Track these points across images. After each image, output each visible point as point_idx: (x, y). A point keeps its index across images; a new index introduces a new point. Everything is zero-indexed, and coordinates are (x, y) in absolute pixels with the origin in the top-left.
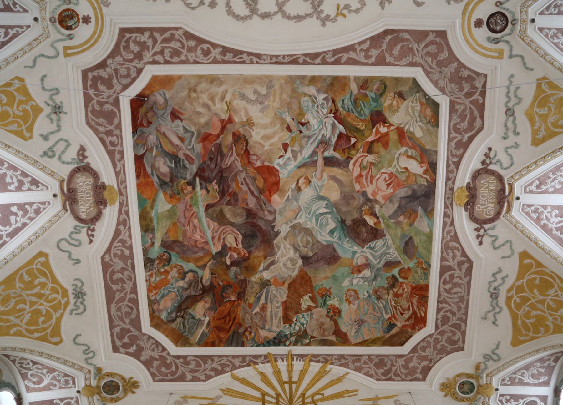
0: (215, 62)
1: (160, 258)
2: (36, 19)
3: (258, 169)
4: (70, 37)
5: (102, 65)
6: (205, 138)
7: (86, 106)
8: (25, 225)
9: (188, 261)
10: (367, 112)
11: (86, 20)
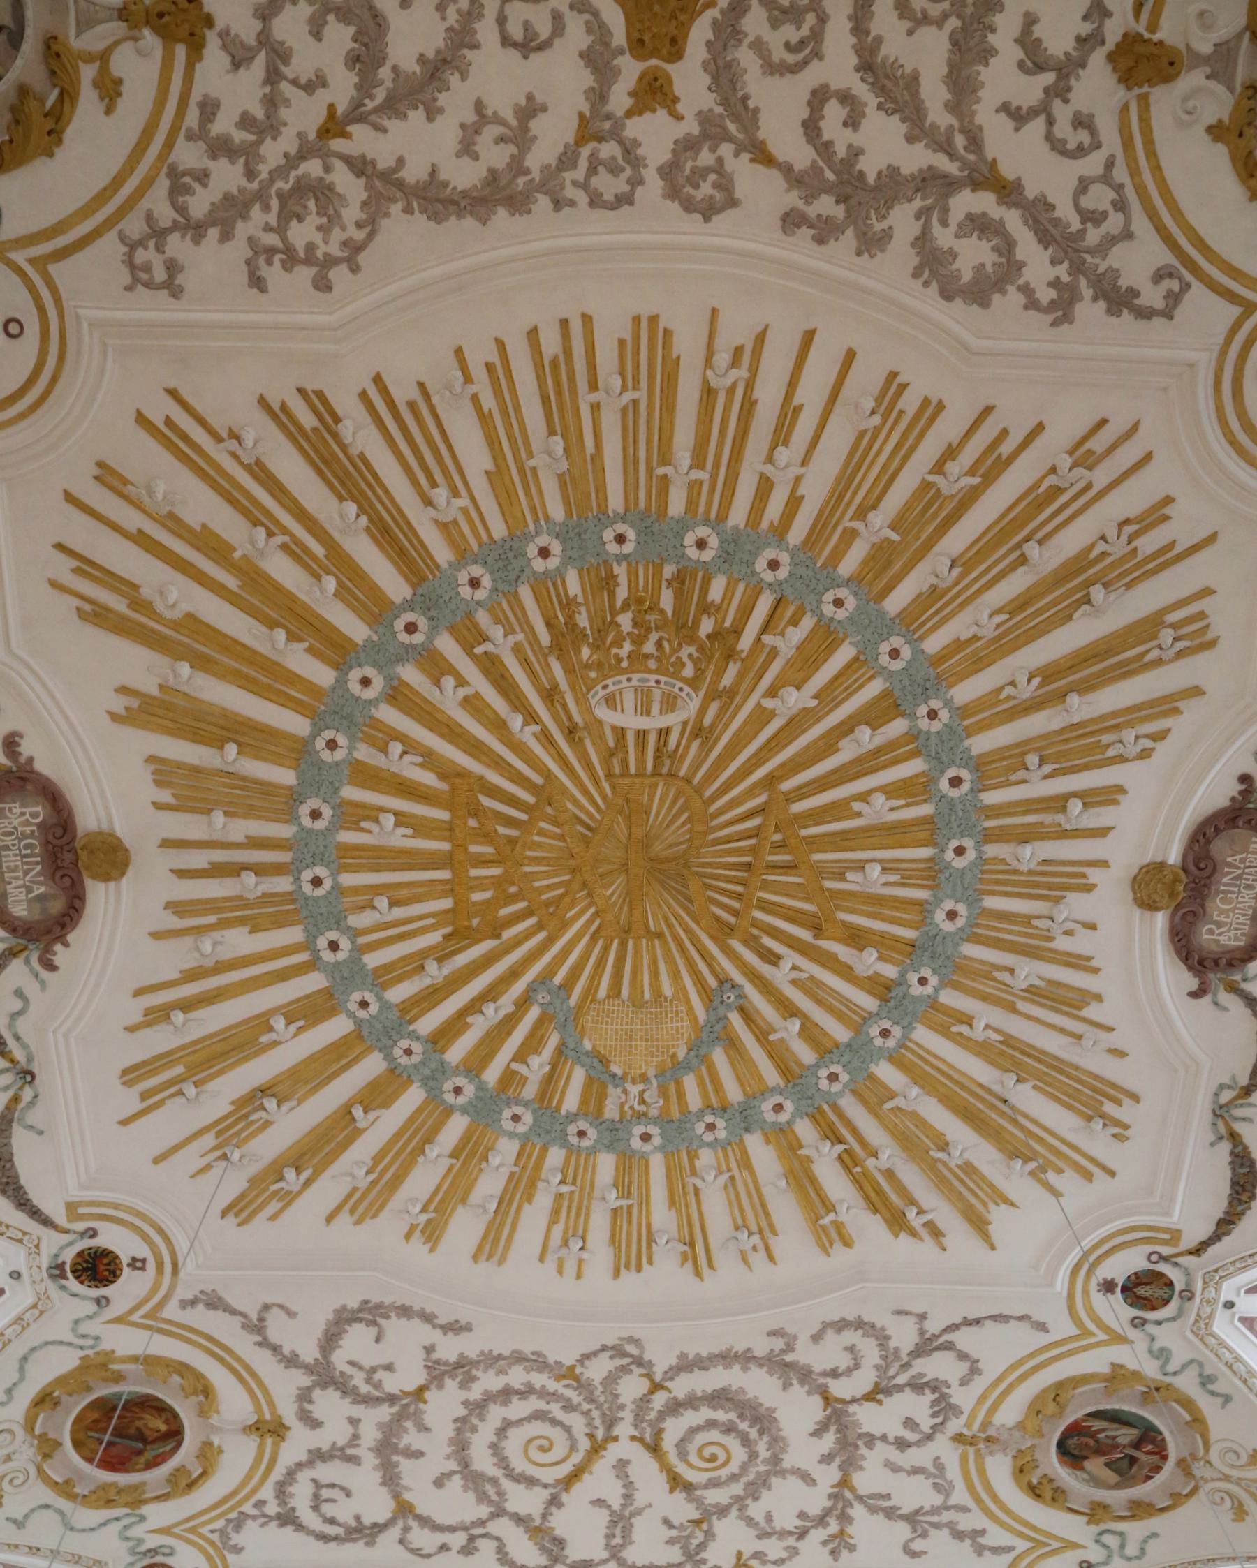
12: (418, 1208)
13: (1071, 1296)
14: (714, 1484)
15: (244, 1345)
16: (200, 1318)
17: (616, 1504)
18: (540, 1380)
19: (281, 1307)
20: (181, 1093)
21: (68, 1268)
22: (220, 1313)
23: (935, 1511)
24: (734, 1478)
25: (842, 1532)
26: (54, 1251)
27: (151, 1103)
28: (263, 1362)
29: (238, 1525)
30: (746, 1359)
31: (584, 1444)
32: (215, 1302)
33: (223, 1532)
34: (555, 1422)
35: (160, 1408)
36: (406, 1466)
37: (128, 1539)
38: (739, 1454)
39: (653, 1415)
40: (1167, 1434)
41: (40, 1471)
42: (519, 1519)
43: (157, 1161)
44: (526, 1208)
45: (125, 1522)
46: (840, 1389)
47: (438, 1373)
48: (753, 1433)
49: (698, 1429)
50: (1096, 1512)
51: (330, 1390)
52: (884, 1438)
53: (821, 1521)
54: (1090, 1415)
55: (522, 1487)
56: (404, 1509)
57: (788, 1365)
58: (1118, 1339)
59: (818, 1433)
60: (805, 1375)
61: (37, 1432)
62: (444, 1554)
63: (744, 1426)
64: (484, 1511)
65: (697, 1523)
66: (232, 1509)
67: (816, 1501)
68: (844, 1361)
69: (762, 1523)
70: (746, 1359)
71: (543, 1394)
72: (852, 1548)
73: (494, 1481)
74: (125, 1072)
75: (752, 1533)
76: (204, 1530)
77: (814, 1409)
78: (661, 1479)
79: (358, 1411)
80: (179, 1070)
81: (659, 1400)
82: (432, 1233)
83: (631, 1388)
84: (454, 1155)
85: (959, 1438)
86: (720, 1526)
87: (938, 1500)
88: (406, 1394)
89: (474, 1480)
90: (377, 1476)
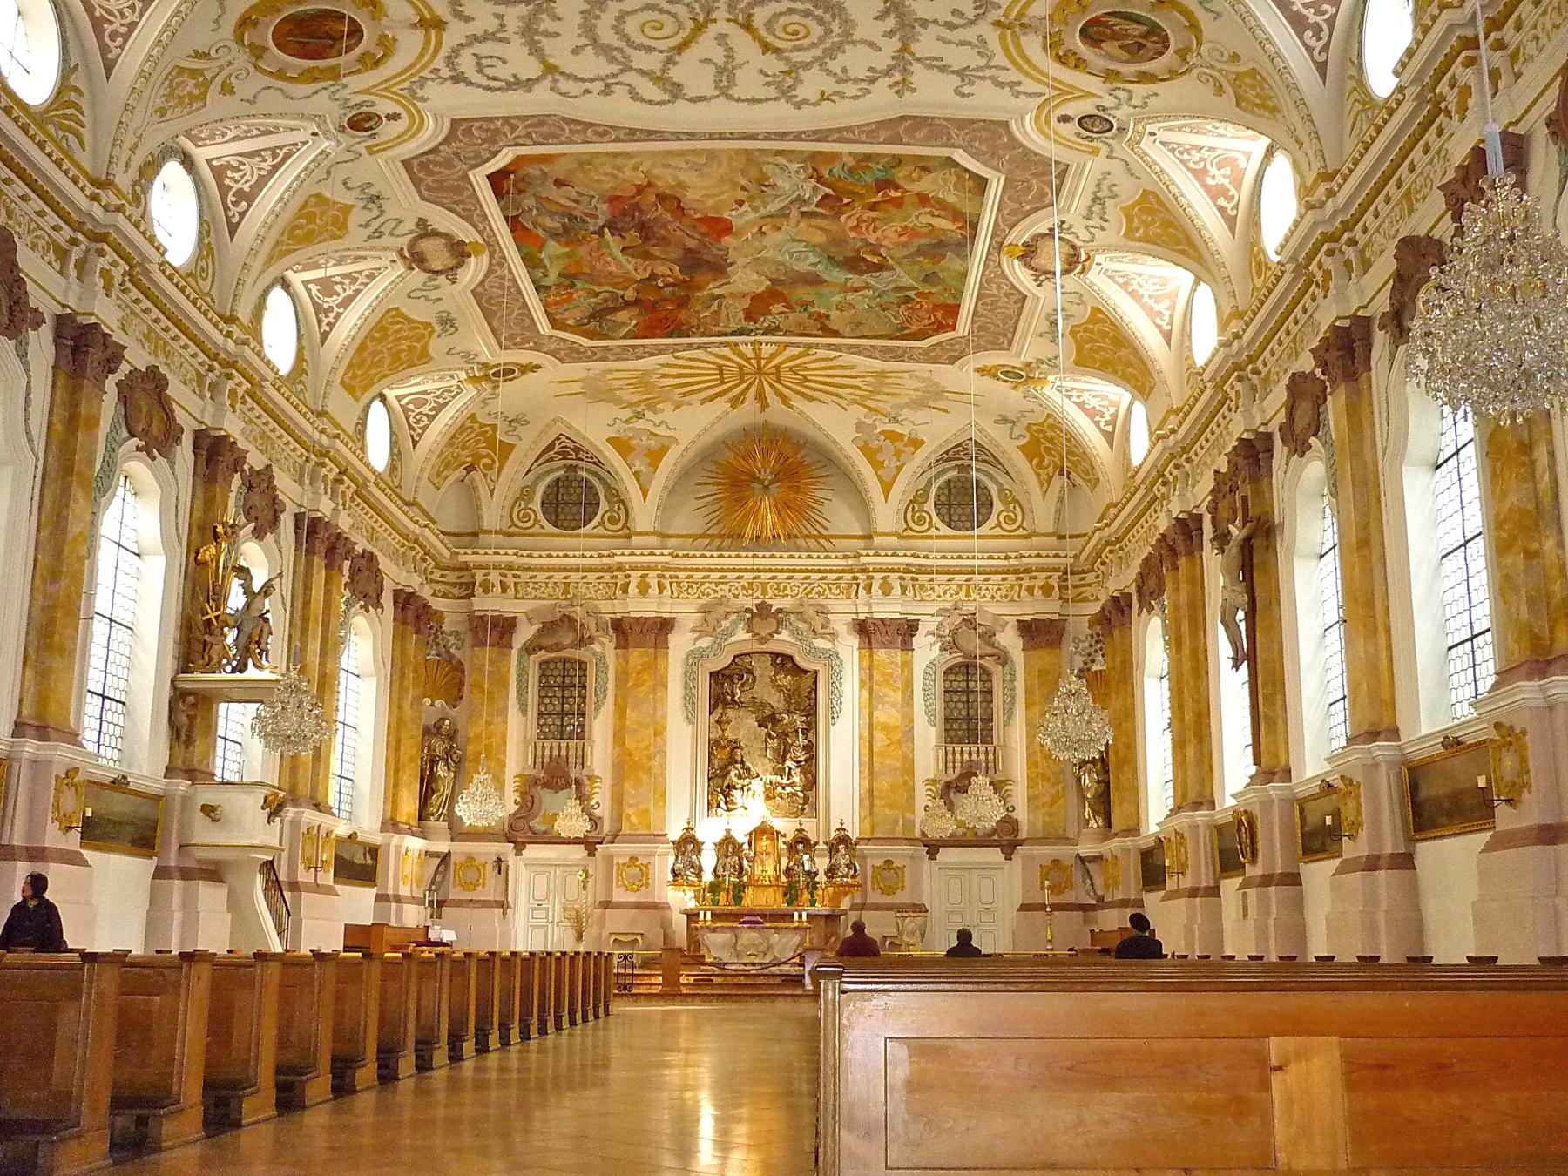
0: (617, 140)
1: (559, 285)
2: (314, 134)
3: (698, 219)
4: (373, 136)
5: (434, 150)
6: (612, 200)
7: (417, 187)
8: (358, 292)
9: (600, 284)
10: (869, 179)
11: (394, 117)
14: (798, 49)
17: (720, 61)
23: (979, 69)
24: (814, 45)
25: (904, 80)
29: (423, 82)
31: (691, 25)
33: (410, 89)
34: (661, 11)
36: (546, 43)
38: (817, 31)
40: (1169, 32)
42: (643, 73)
45: (332, 89)
48: (827, 17)
49: (781, 14)
50: (1110, 76)
52: (935, 21)
53: (888, 72)
54: (1109, 14)
56: (550, 69)
59: (882, 16)
63: (819, 12)
64: (615, 68)
65: (787, 73)
66: (412, 75)
67: (883, 60)
69: (839, 73)
72: (914, 90)
73: (620, 50)
76: (394, 89)
78: (755, 48)
85: (997, 24)
86: (804, 75)
87: (983, 62)
89: (605, 50)
90: (526, 49)
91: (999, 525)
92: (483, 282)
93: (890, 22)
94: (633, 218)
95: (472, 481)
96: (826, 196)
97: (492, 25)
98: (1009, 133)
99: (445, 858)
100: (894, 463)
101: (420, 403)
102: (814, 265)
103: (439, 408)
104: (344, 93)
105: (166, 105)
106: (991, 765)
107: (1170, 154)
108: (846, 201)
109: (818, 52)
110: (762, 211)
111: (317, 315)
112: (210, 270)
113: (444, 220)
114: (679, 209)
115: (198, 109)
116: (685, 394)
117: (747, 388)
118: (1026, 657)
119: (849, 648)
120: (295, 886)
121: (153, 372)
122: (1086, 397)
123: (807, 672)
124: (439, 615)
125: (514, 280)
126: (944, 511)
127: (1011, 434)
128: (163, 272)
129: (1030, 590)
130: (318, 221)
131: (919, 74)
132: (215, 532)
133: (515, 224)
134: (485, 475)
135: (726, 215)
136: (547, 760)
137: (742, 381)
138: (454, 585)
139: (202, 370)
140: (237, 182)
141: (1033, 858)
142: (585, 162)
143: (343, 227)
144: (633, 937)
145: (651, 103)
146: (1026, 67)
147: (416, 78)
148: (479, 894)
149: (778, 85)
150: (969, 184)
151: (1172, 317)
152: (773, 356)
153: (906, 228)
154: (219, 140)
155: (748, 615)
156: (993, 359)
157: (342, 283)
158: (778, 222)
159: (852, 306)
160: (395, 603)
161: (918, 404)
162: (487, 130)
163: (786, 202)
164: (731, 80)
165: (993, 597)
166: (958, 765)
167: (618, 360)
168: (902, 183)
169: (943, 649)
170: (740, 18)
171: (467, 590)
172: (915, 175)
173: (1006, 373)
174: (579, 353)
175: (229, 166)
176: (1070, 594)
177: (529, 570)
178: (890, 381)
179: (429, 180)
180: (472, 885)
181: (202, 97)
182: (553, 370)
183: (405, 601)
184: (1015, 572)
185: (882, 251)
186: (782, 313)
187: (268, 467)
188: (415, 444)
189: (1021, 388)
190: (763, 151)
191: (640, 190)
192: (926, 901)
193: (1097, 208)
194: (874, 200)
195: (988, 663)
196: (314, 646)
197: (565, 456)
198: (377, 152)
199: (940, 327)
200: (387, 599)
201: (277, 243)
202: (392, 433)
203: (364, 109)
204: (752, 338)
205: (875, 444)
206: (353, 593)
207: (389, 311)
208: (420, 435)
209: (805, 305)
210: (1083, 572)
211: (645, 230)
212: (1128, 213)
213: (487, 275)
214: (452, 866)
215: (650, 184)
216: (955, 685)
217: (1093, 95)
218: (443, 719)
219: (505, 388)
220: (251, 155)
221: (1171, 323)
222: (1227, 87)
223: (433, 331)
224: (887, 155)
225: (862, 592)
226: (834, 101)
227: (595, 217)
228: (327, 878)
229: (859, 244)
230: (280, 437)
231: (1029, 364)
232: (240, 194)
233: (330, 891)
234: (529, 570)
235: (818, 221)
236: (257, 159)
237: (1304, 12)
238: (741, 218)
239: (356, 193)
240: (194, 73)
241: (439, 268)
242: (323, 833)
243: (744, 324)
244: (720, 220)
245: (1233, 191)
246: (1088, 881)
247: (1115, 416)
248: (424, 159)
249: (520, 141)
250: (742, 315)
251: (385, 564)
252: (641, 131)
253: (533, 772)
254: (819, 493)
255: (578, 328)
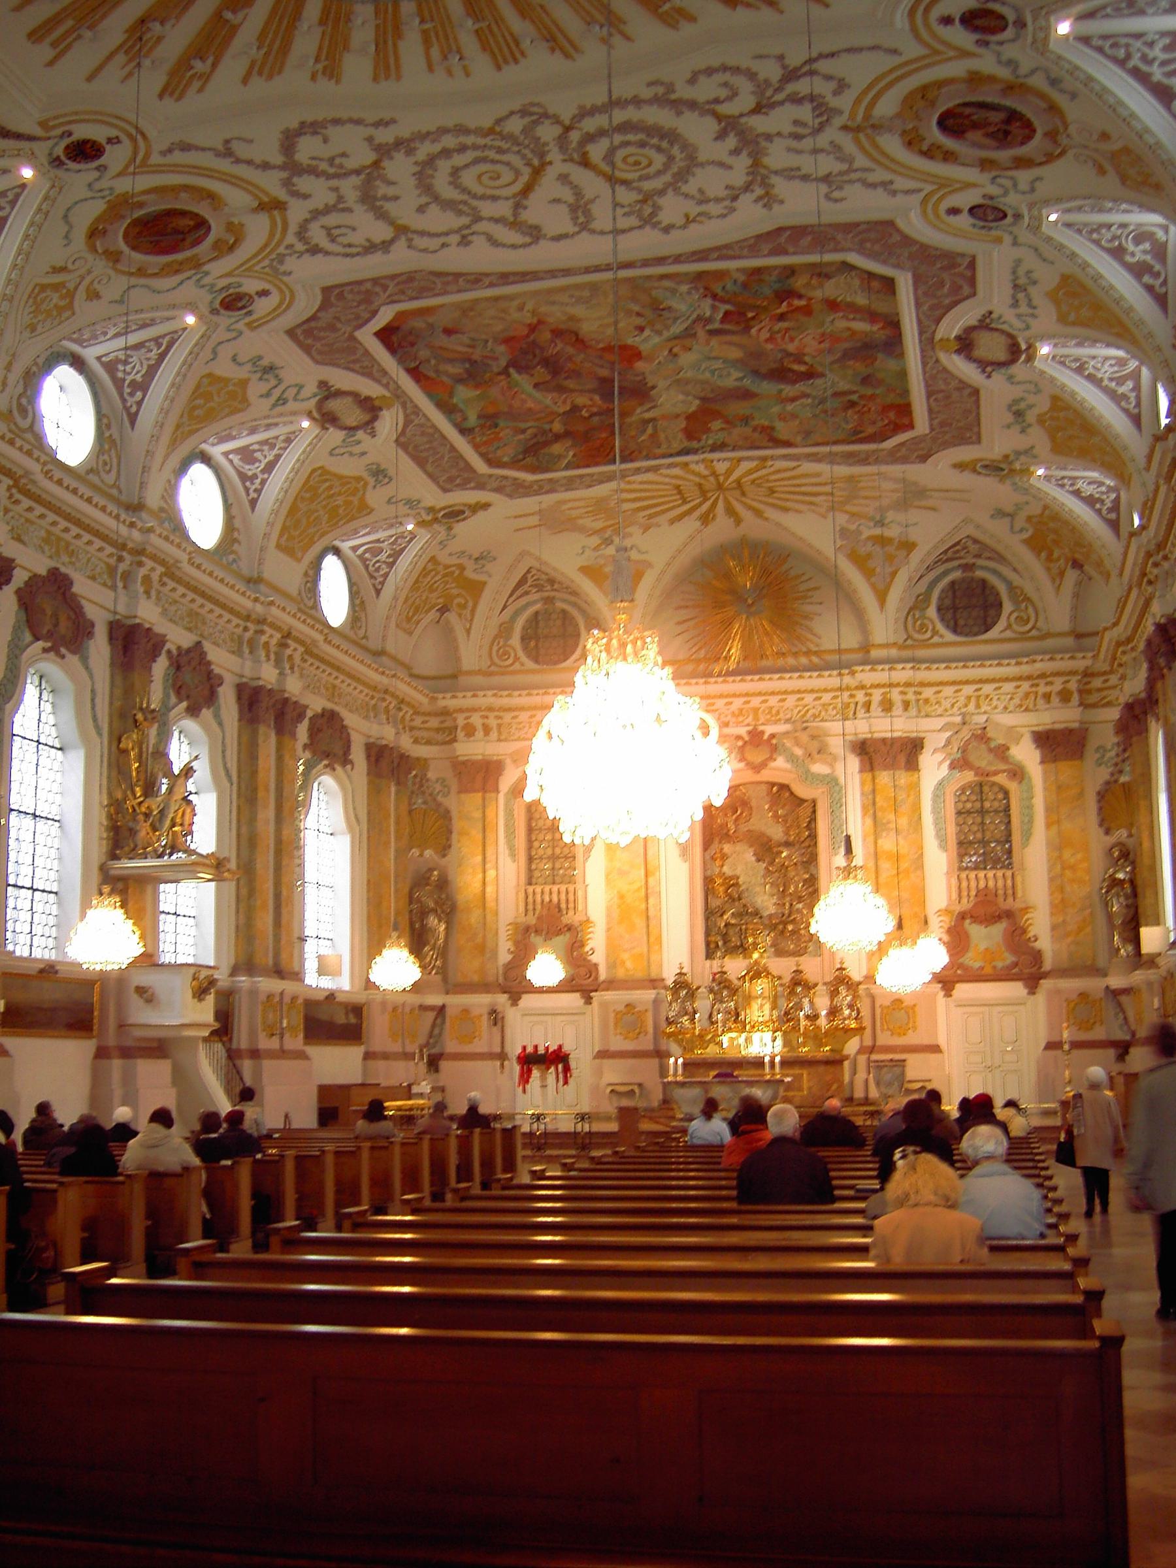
0: (491, 285)
1: (482, 426)
3: (603, 349)
4: (250, 313)
5: (313, 318)
6: (507, 341)
8: (278, 457)
10: (767, 291)
11: (264, 293)
12: (312, 61)
13: (914, 30)
14: (647, 178)
15: (225, 165)
16: (178, 157)
17: (571, 199)
18: (470, 140)
19: (239, 139)
20: (79, 37)
21: (63, 158)
22: (193, 152)
23: (841, 173)
24: (659, 173)
25: (767, 193)
26: (47, 152)
27: (61, 48)
28: (242, 171)
29: (281, 259)
30: (637, 102)
31: (526, 172)
32: (186, 147)
34: (493, 162)
35: (183, 213)
36: (389, 206)
37: (203, 286)
38: (659, 160)
39: (574, 145)
41: (116, 270)
43: (90, 78)
44: (402, 45)
45: (195, 278)
46: (725, 109)
47: (384, 151)
50: (985, 165)
51: (305, 176)
52: (779, 134)
53: (747, 188)
54: (959, 105)
55: (489, 202)
56: (401, 230)
57: (674, 101)
58: (964, 54)
59: (721, 136)
60: (692, 105)
61: (100, 251)
62: (446, 250)
64: (465, 220)
66: (270, 253)
67: (738, 177)
68: (723, 93)
69: (698, 196)
70: (637, 102)
71: (475, 147)
73: (465, 203)
74: (30, 35)
75: (691, 203)
77: (711, 126)
79: (334, 183)
80: (70, 23)
81: (575, 136)
82: (332, 71)
83: (547, 132)
84: (322, 22)
86: (662, 201)
87: (845, 167)
88: (365, 167)
89: (448, 205)
90: (370, 216)
91: (1009, 627)
92: (403, 433)
93: (731, 141)
94: (535, 356)
95: (448, 622)
96: (727, 314)
97: (331, 199)
98: (898, 231)
99: (441, 1010)
100: (889, 570)
101: (377, 552)
102: (741, 379)
103: (396, 554)
104: (207, 280)
105: (35, 321)
106: (1010, 892)
107: (1077, 236)
108: (750, 315)
109: (667, 177)
110: (666, 334)
111: (244, 483)
112: (115, 461)
113: (343, 379)
114: (579, 341)
115: (68, 318)
116: (650, 517)
117: (714, 505)
118: (1045, 773)
119: (850, 770)
120: (255, 1054)
121: (54, 573)
122: (1080, 484)
123: (805, 801)
124: (423, 763)
125: (434, 426)
126: (949, 615)
127: (1012, 527)
128: (51, 478)
129: (1047, 697)
130: (216, 398)
131: (780, 186)
132: (136, 721)
133: (416, 374)
134: (460, 615)
135: (630, 341)
136: (539, 907)
137: (706, 499)
138: (438, 730)
139: (112, 561)
140: (129, 374)
141: (1058, 992)
142: (467, 309)
143: (245, 400)
144: (630, 1088)
145: (514, 247)
146: (892, 166)
147: (274, 256)
148: (479, 1046)
149: (640, 217)
150: (875, 284)
151: (1138, 398)
152: (729, 473)
153: (823, 335)
154: (102, 339)
155: (740, 743)
156: (966, 453)
157: (261, 450)
158: (687, 342)
159: (794, 416)
160: (368, 757)
161: (903, 504)
162: (359, 293)
163: (689, 322)
164: (587, 213)
165: (1005, 708)
166: (973, 893)
167: (566, 490)
168: (803, 291)
169: (953, 766)
170: (575, 156)
171: (449, 735)
172: (814, 282)
173: (986, 467)
174: (526, 488)
175: (117, 361)
176: (1093, 698)
177: (510, 710)
178: (861, 484)
179: (318, 345)
180: (470, 1038)
181: (70, 306)
182: (503, 506)
183: (378, 754)
184: (1029, 678)
185: (807, 359)
186: (722, 429)
187: (199, 644)
188: (378, 592)
189: (1008, 482)
190: (649, 278)
191: (533, 328)
192: (942, 1041)
193: (1021, 296)
194: (779, 311)
195: (1001, 779)
196: (267, 814)
197: (540, 588)
198: (256, 328)
199: (897, 428)
200: (358, 754)
201: (178, 427)
202: (352, 584)
203: (231, 291)
204: (702, 456)
205: (862, 551)
206: (314, 753)
207: (314, 471)
208: (382, 583)
209: (746, 420)
210: (1105, 673)
211: (554, 366)
212: (1052, 296)
213: (406, 426)
214: (448, 1020)
215: (540, 322)
216: (969, 805)
217: (974, 185)
218: (431, 870)
219: (460, 528)
220: (138, 347)
221: (1138, 405)
222: (1108, 166)
223: (366, 484)
224: (775, 267)
225: (861, 713)
226: (701, 222)
227: (496, 359)
228: (295, 1042)
229: (780, 356)
230: (211, 611)
231: (1006, 457)
232: (133, 384)
233: (301, 1055)
234: (510, 710)
235: (728, 338)
236: (143, 350)
237: (1166, 81)
238: (648, 342)
239: (249, 367)
240: (56, 287)
241: (354, 424)
242: (287, 999)
243: (686, 444)
244: (624, 348)
245: (1157, 267)
246: (1121, 1016)
247: (1117, 501)
248: (305, 327)
249: (395, 298)
250: (680, 435)
251: (351, 720)
252: (515, 274)
253: (522, 919)
254: (808, 608)
255: (515, 464)
